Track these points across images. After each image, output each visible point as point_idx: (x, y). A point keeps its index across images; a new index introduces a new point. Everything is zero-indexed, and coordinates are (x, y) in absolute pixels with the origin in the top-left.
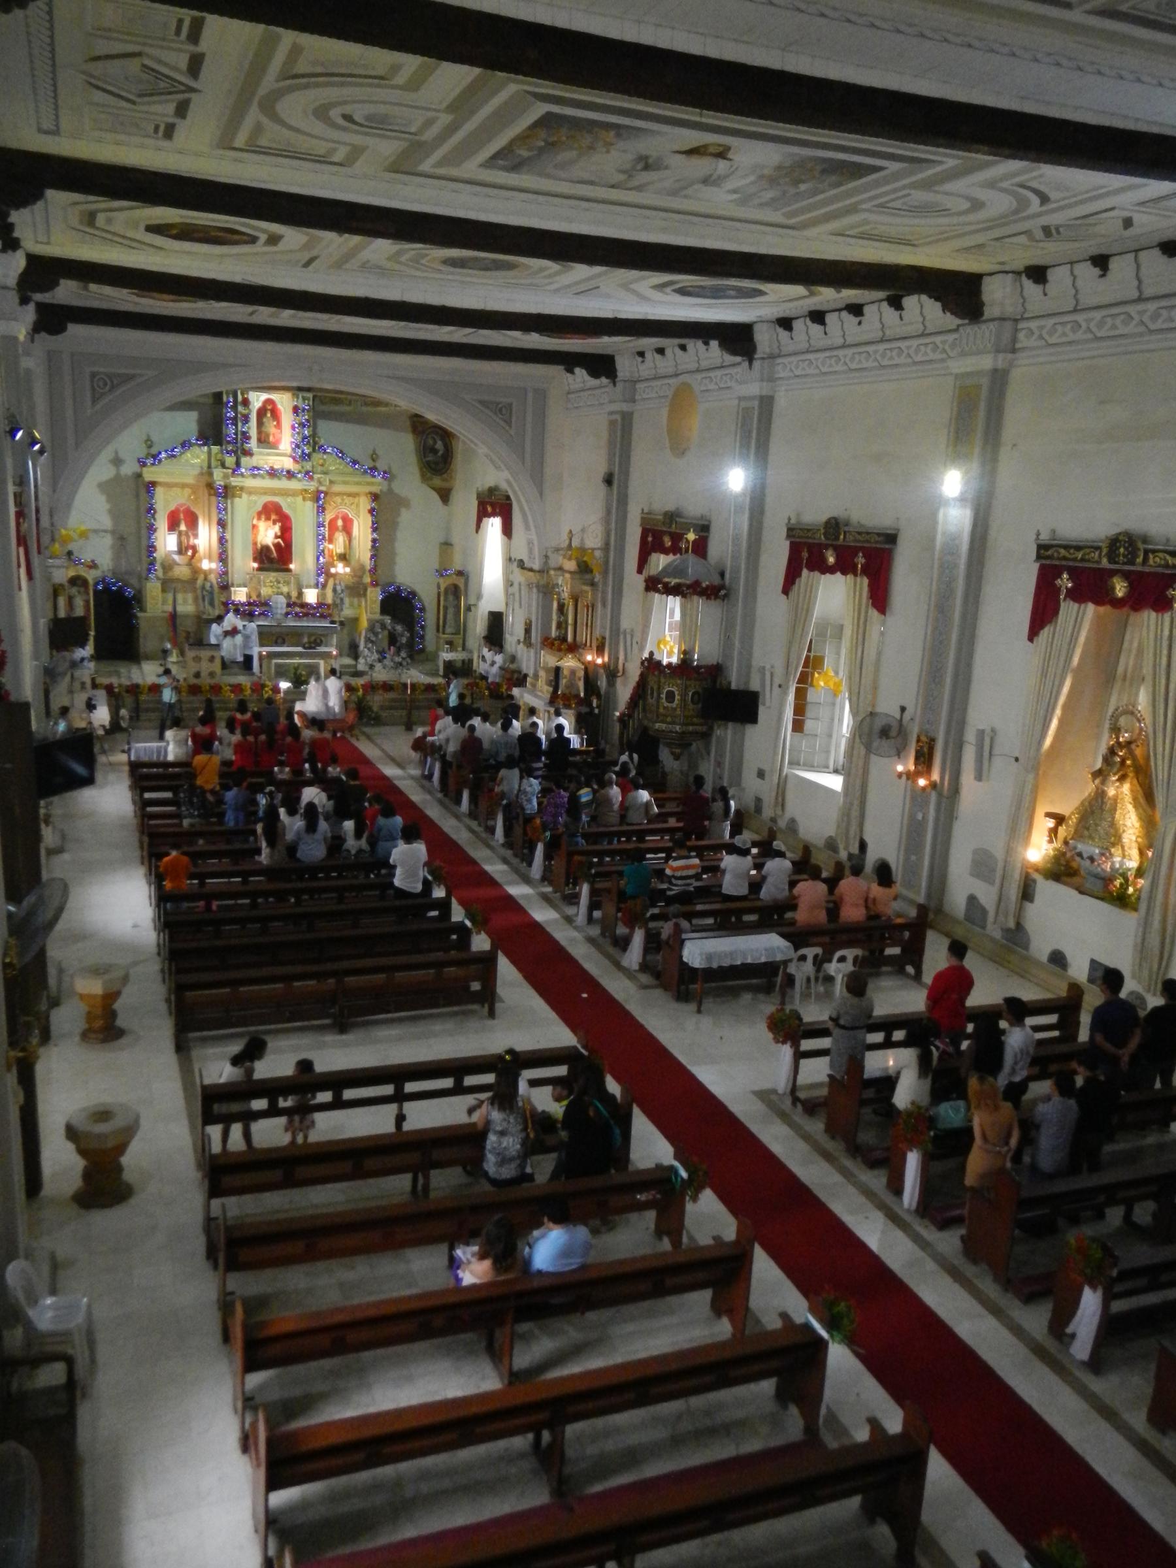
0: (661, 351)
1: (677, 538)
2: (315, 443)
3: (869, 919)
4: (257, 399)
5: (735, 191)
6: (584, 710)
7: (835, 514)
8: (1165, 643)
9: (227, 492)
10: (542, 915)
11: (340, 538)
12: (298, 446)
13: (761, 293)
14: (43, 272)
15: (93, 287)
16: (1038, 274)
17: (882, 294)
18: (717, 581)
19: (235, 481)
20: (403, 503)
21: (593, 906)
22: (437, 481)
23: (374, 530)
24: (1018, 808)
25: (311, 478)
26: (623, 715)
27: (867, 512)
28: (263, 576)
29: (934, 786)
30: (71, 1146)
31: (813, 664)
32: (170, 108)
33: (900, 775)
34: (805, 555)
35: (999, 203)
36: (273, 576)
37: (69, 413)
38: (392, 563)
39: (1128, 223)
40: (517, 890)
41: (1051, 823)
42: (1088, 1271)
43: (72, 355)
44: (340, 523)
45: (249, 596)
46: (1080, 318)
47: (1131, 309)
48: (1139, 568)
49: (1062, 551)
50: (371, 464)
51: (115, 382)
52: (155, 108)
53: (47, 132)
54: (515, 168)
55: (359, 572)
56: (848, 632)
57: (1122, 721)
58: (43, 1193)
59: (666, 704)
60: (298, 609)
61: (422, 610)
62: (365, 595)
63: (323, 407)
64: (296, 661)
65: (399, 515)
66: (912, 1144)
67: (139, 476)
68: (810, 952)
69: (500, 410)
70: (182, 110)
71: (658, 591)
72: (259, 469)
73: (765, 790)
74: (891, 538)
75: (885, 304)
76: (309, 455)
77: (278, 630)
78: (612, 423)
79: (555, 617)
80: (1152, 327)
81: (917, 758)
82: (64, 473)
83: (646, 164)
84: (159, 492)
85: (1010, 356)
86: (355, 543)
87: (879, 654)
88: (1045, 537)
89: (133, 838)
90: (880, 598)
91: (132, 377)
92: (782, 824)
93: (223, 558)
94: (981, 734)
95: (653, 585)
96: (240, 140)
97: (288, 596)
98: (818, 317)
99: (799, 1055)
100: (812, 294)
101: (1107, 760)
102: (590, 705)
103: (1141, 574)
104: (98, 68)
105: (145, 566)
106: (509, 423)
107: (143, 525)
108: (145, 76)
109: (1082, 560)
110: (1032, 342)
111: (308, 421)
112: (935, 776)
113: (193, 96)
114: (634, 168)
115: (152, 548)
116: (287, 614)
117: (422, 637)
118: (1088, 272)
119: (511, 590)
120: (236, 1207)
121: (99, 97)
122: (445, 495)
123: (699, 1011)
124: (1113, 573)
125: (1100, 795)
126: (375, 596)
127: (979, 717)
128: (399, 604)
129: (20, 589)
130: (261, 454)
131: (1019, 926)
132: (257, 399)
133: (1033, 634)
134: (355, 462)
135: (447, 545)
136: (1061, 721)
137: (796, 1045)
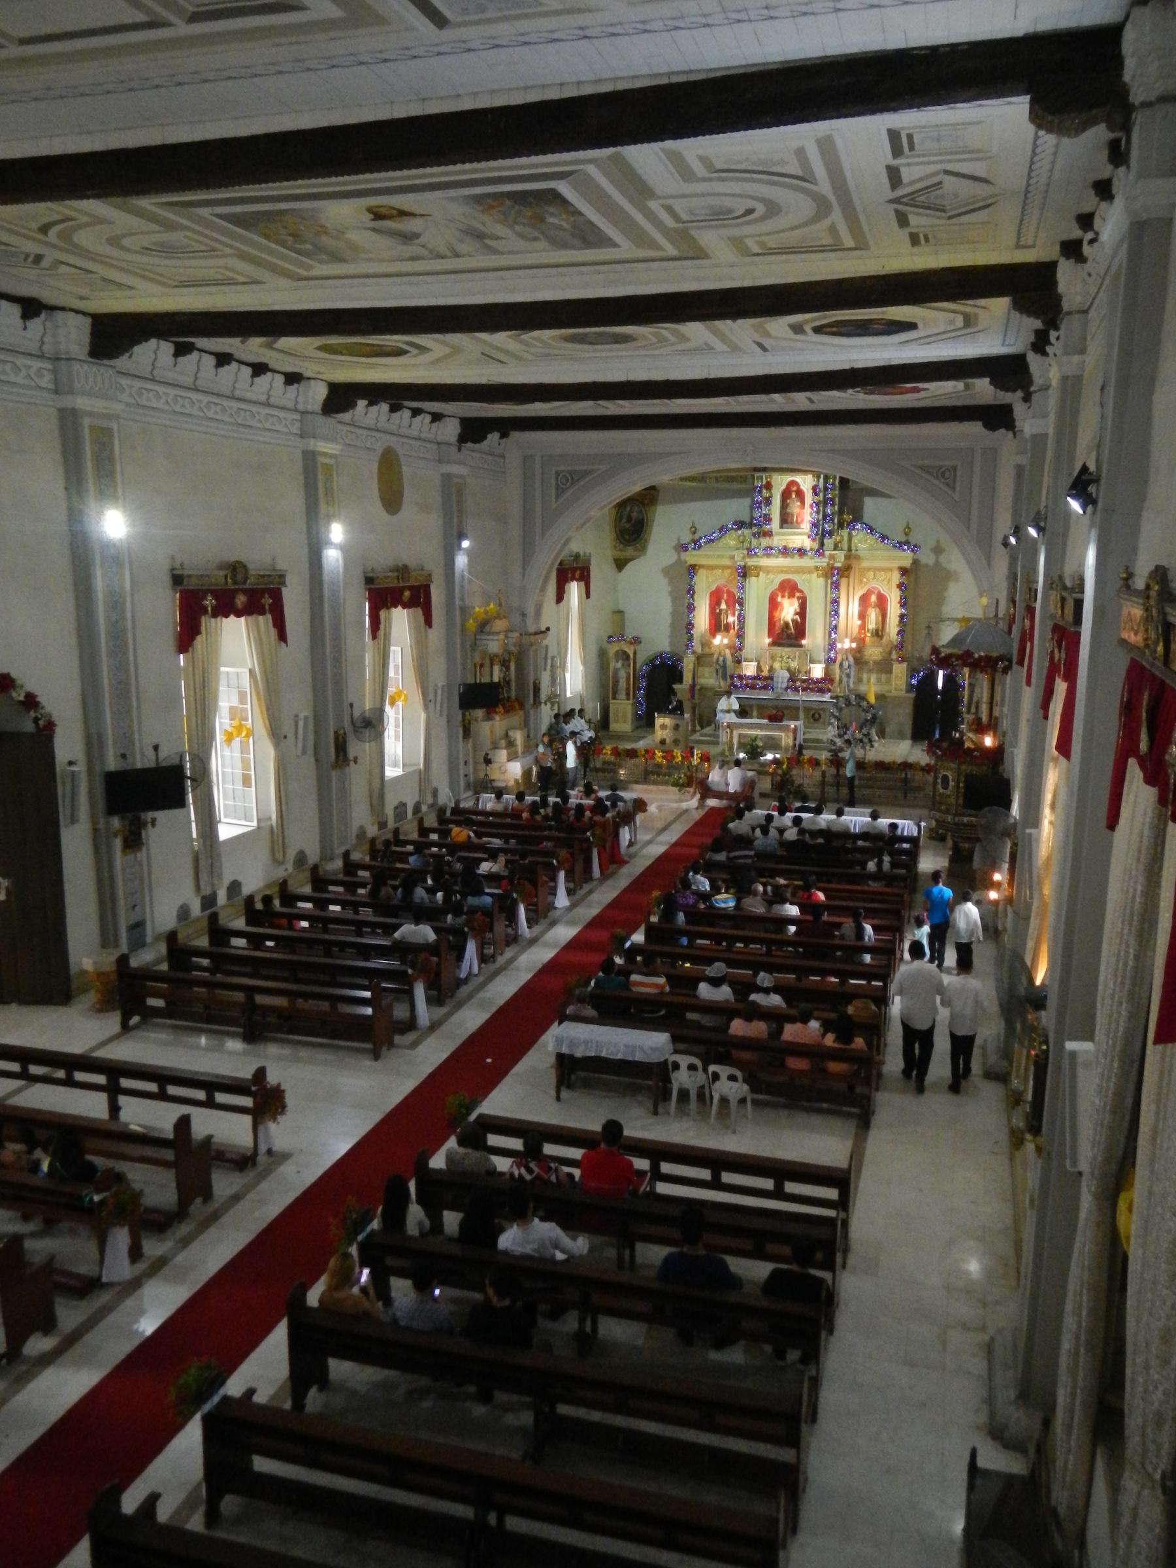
4: (780, 482)
9: (744, 573)
11: (873, 615)
12: (815, 525)
13: (912, 326)
19: (751, 562)
37: (538, 509)
44: (873, 598)
45: (759, 668)
50: (903, 539)
51: (576, 478)
59: (941, 791)
62: (890, 672)
64: (759, 732)
65: (946, 589)
69: (943, 474)
72: (771, 549)
76: (831, 534)
77: (776, 703)
85: (1076, 359)
91: (590, 472)
106: (953, 489)
111: (831, 499)
116: (787, 688)
130: (783, 534)
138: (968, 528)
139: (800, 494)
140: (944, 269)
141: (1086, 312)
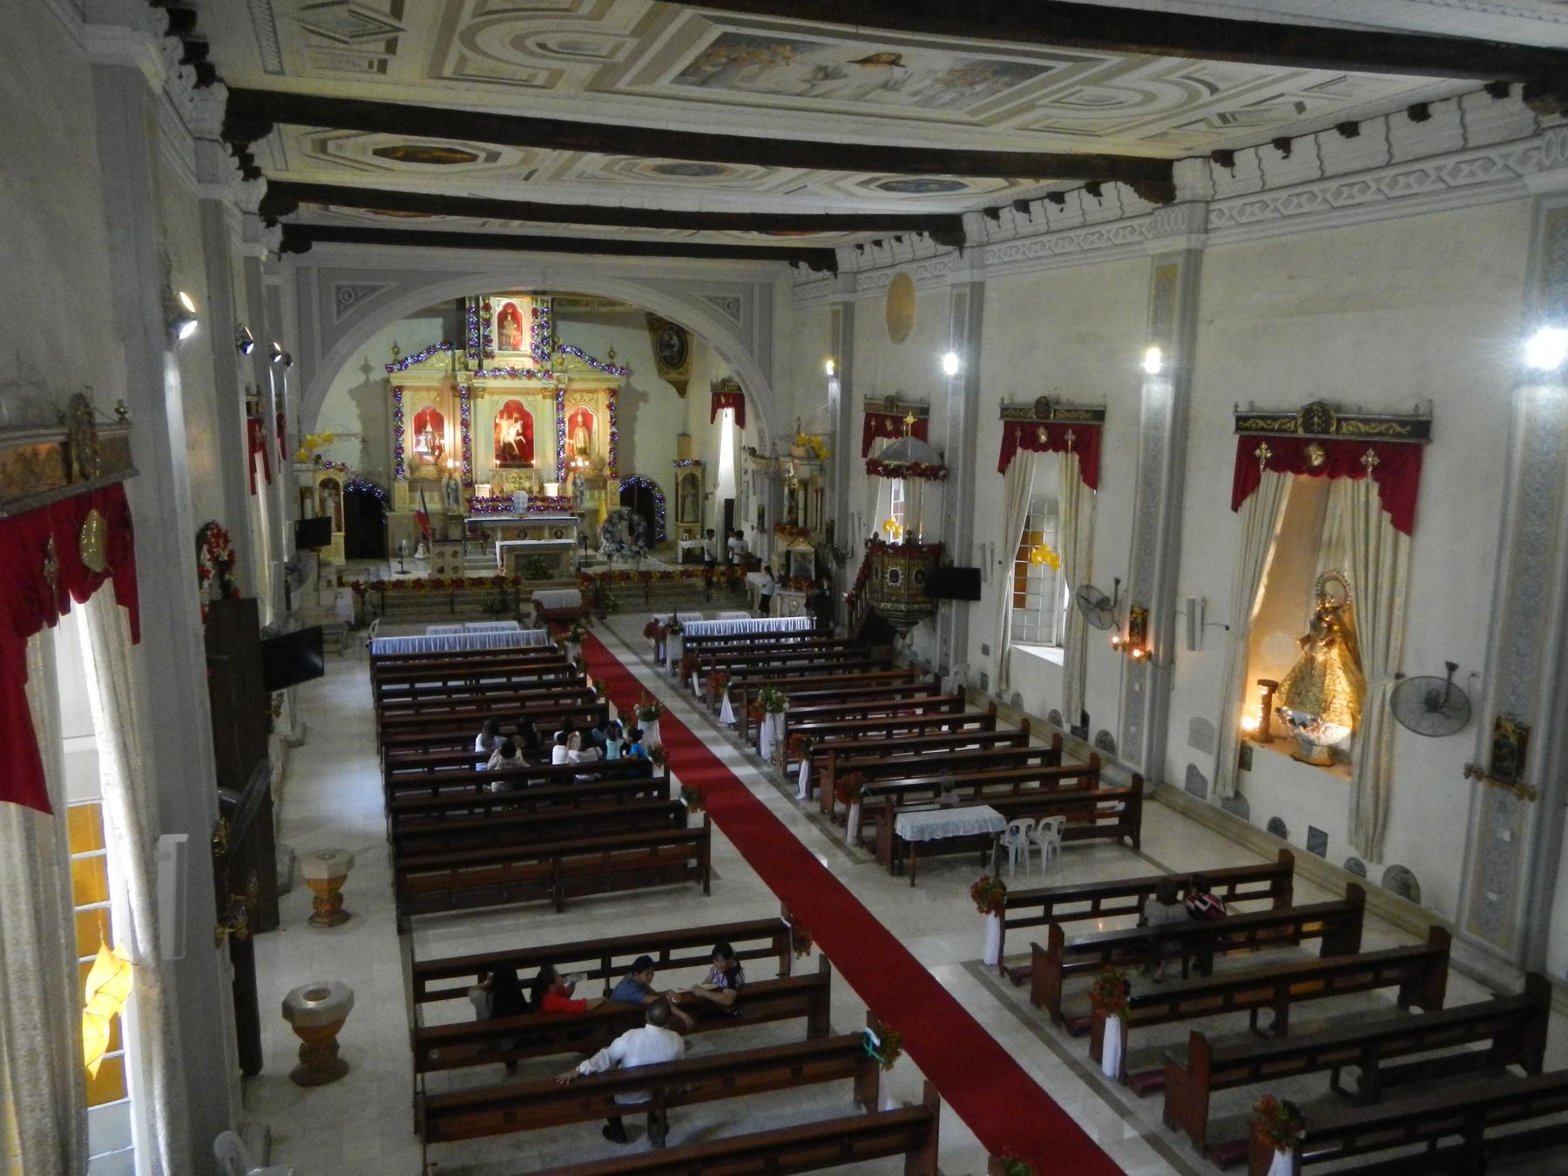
0: (878, 243)
1: (898, 421)
2: (554, 343)
3: (1064, 785)
5: (915, 94)
6: (816, 591)
7: (1045, 393)
8: (1362, 508)
9: (470, 394)
10: (766, 795)
11: (580, 433)
12: (537, 347)
13: (963, 186)
14: (282, 197)
15: (333, 208)
16: (1225, 157)
17: (1081, 183)
18: (936, 462)
19: (477, 383)
20: (643, 397)
21: (813, 782)
22: (674, 375)
23: (613, 424)
24: (1231, 677)
25: (551, 377)
26: (851, 596)
27: (1076, 391)
28: (505, 472)
29: (1149, 656)
30: (288, 1026)
31: (1031, 537)
32: (382, 46)
33: (1116, 647)
34: (1019, 434)
35: (1170, 95)
36: (514, 472)
37: (317, 327)
38: (632, 454)
39: (1300, 107)
40: (743, 772)
41: (1264, 691)
42: (1275, 1132)
43: (319, 271)
44: (580, 419)
45: (492, 492)
46: (1266, 197)
47: (1315, 188)
48: (1334, 437)
49: (1261, 423)
50: (609, 361)
52: (370, 47)
53: (276, 73)
54: (703, 83)
55: (598, 465)
56: (1062, 507)
57: (1330, 587)
58: (262, 1072)
60: (539, 503)
61: (662, 499)
62: (604, 487)
63: (561, 310)
66: (1110, 1009)
67: (387, 381)
68: (1023, 823)
70: (391, 47)
71: (878, 473)
73: (990, 666)
74: (1100, 415)
75: (1084, 191)
76: (549, 356)
78: (835, 314)
79: (786, 503)
80: (1336, 204)
81: (1131, 630)
82: (311, 381)
83: (826, 73)
84: (406, 397)
85: (1203, 236)
86: (595, 437)
87: (1092, 529)
88: (1243, 409)
89: (371, 728)
90: (1091, 473)
91: (374, 289)
92: (1007, 699)
93: (467, 456)
94: (1192, 603)
95: (874, 468)
96: (448, 70)
97: (530, 491)
98: (1023, 205)
99: (1006, 925)
100: (1012, 185)
101: (1316, 623)
102: (821, 587)
103: (1337, 443)
104: (310, 15)
105: (393, 467)
106: (738, 318)
107: (392, 428)
108: (352, 20)
109: (1279, 430)
110: (1224, 222)
112: (1150, 647)
113: (400, 35)
114: (814, 77)
115: (399, 450)
117: (663, 527)
118: (1271, 154)
119: (745, 478)
120: (437, 1081)
121: (315, 40)
122: (682, 389)
123: (913, 885)
124: (1308, 442)
125: (1311, 660)
126: (615, 487)
127: (1192, 584)
128: (639, 497)
129: (254, 492)
131: (1238, 795)
132: (498, 304)
133: (1236, 506)
134: (593, 360)
135: (684, 436)
136: (1267, 588)
137: (1000, 914)
138: (751, 353)
139: (516, 317)
140: (1099, 155)
141: (1208, 202)
